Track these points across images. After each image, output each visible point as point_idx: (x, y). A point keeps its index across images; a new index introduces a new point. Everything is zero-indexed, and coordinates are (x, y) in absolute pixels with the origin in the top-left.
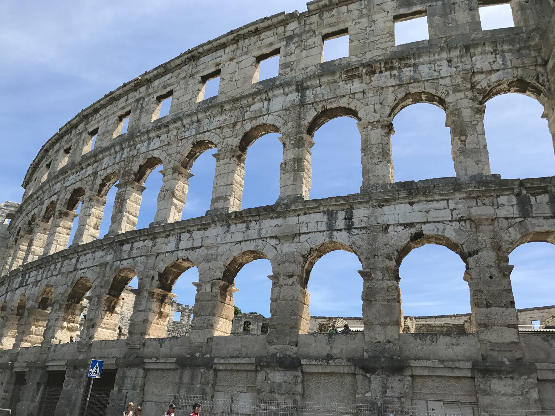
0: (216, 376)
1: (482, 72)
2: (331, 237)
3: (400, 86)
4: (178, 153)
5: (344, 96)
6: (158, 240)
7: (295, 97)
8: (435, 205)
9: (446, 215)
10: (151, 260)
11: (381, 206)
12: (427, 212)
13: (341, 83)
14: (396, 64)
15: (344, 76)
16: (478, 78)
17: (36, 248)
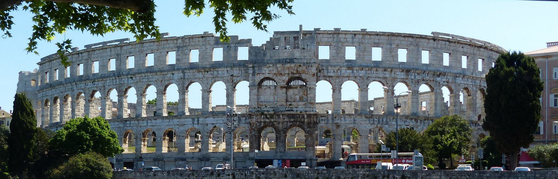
0: (165, 163)
1: (235, 76)
2: (193, 126)
3: (213, 78)
4: (141, 87)
5: (197, 78)
6: (140, 122)
7: (181, 75)
8: (219, 119)
9: (222, 122)
10: (139, 128)
11: (206, 118)
12: (217, 121)
13: (196, 73)
14: (212, 70)
15: (197, 71)
16: (234, 78)
17: (77, 113)
